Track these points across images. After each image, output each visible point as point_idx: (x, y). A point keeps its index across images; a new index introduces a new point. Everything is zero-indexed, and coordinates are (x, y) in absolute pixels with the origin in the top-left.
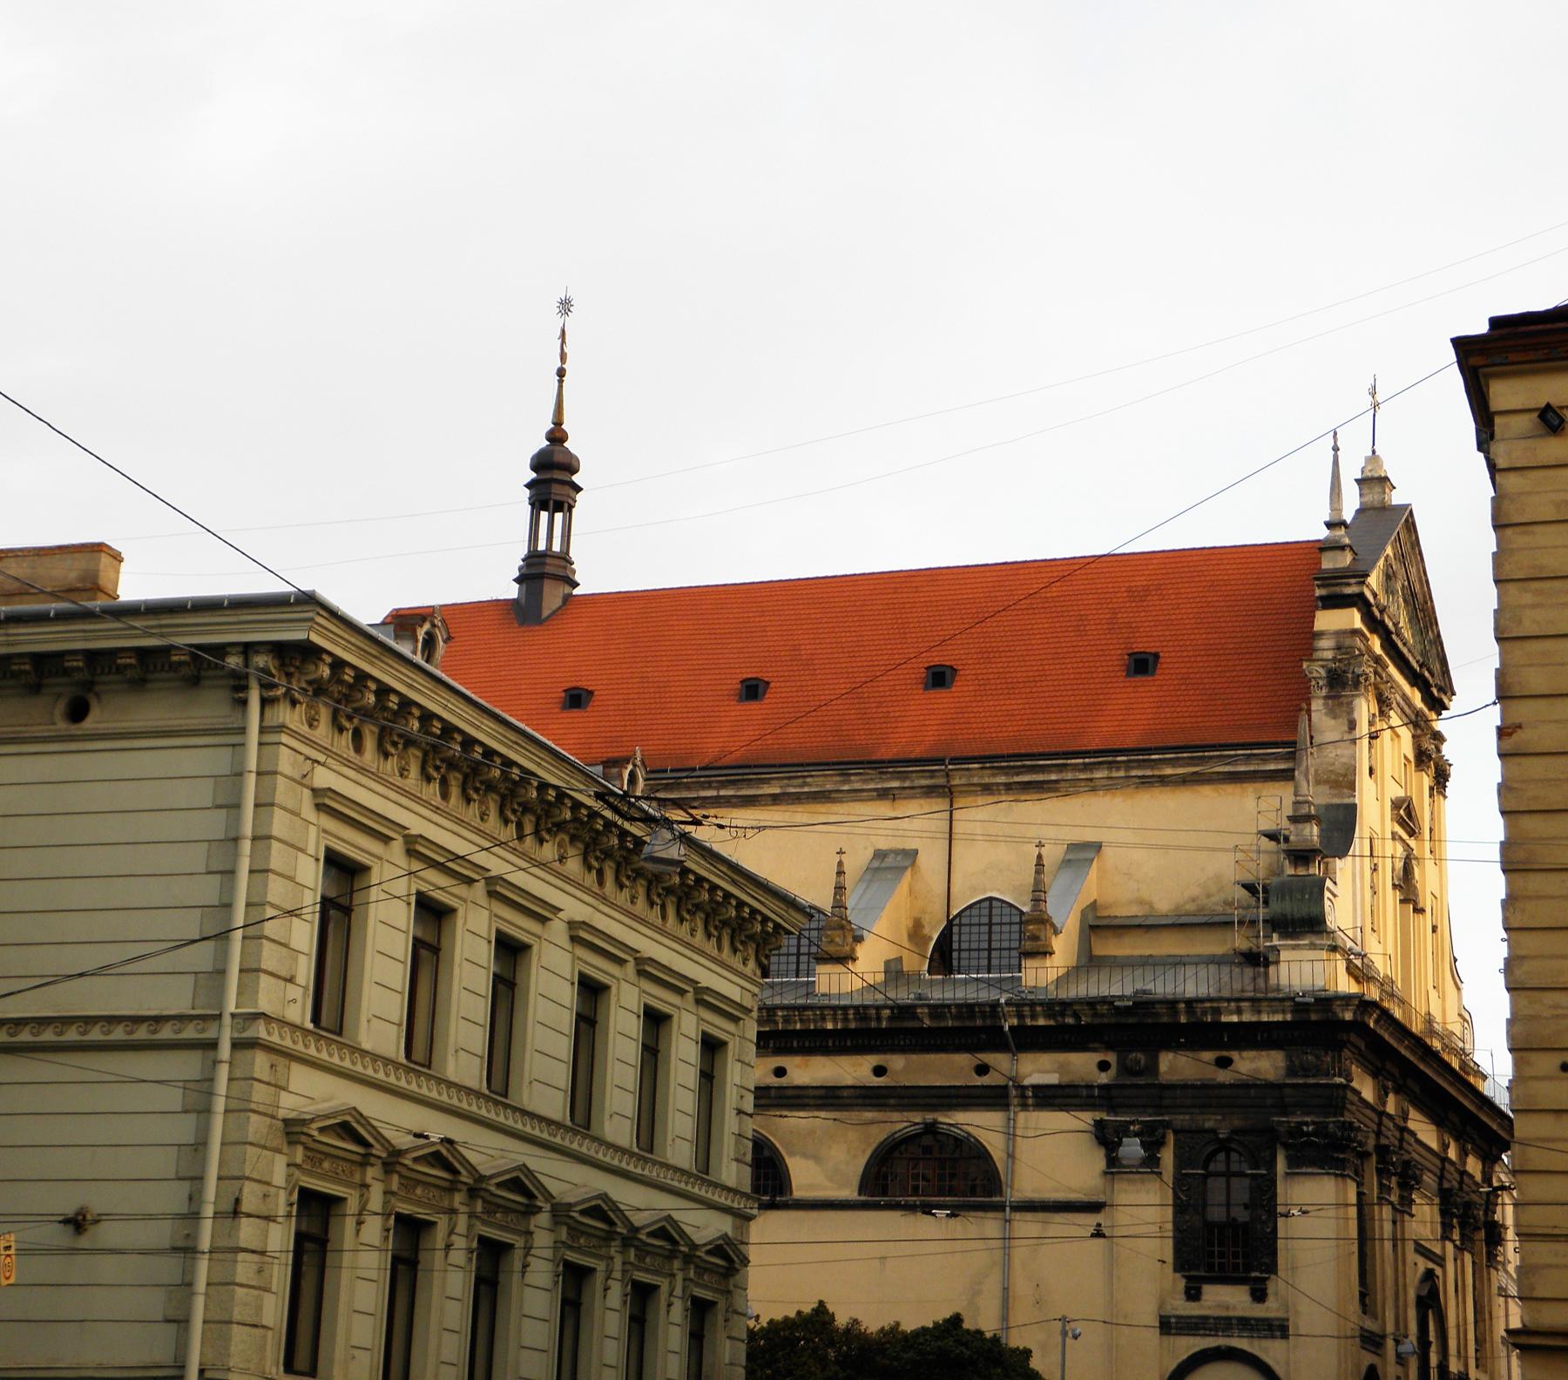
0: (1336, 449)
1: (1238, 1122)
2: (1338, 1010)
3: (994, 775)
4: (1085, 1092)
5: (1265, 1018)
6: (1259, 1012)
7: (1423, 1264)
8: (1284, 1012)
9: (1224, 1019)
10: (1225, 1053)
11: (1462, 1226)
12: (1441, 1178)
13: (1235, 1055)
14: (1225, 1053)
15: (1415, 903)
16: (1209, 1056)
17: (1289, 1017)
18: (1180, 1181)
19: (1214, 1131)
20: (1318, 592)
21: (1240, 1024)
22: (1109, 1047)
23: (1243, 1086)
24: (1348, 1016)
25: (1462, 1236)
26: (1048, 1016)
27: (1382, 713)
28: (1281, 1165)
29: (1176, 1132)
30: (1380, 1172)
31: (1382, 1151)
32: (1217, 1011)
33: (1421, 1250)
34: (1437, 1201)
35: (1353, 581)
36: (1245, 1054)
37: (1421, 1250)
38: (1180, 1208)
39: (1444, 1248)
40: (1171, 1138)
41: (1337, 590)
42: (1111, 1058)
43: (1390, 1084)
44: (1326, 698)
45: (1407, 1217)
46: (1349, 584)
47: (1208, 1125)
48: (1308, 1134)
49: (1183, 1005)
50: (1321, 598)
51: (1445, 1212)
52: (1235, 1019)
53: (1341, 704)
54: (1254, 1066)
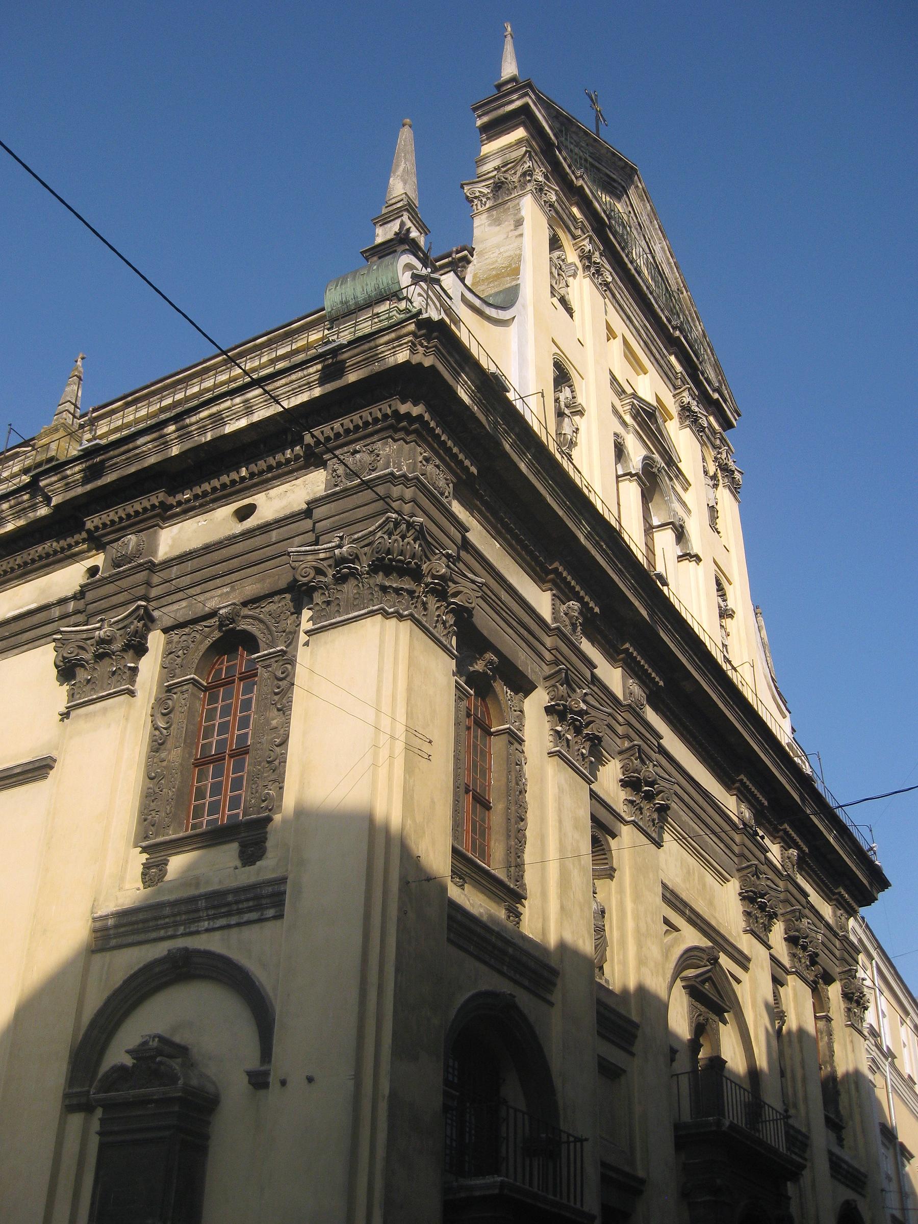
1: (251, 589)
3: (136, 411)
4: (56, 612)
7: (691, 938)
8: (309, 386)
9: (228, 429)
13: (259, 499)
16: (225, 512)
17: (317, 392)
18: (163, 706)
19: (213, 614)
20: (479, 123)
21: (252, 426)
22: (97, 543)
23: (265, 528)
24: (402, 356)
26: (18, 515)
29: (165, 631)
32: (218, 420)
33: (672, 898)
35: (515, 96)
38: (157, 745)
40: (156, 640)
41: (501, 111)
42: (99, 560)
44: (490, 209)
47: (211, 604)
48: (341, 561)
50: (485, 128)
52: (243, 423)
53: (505, 211)
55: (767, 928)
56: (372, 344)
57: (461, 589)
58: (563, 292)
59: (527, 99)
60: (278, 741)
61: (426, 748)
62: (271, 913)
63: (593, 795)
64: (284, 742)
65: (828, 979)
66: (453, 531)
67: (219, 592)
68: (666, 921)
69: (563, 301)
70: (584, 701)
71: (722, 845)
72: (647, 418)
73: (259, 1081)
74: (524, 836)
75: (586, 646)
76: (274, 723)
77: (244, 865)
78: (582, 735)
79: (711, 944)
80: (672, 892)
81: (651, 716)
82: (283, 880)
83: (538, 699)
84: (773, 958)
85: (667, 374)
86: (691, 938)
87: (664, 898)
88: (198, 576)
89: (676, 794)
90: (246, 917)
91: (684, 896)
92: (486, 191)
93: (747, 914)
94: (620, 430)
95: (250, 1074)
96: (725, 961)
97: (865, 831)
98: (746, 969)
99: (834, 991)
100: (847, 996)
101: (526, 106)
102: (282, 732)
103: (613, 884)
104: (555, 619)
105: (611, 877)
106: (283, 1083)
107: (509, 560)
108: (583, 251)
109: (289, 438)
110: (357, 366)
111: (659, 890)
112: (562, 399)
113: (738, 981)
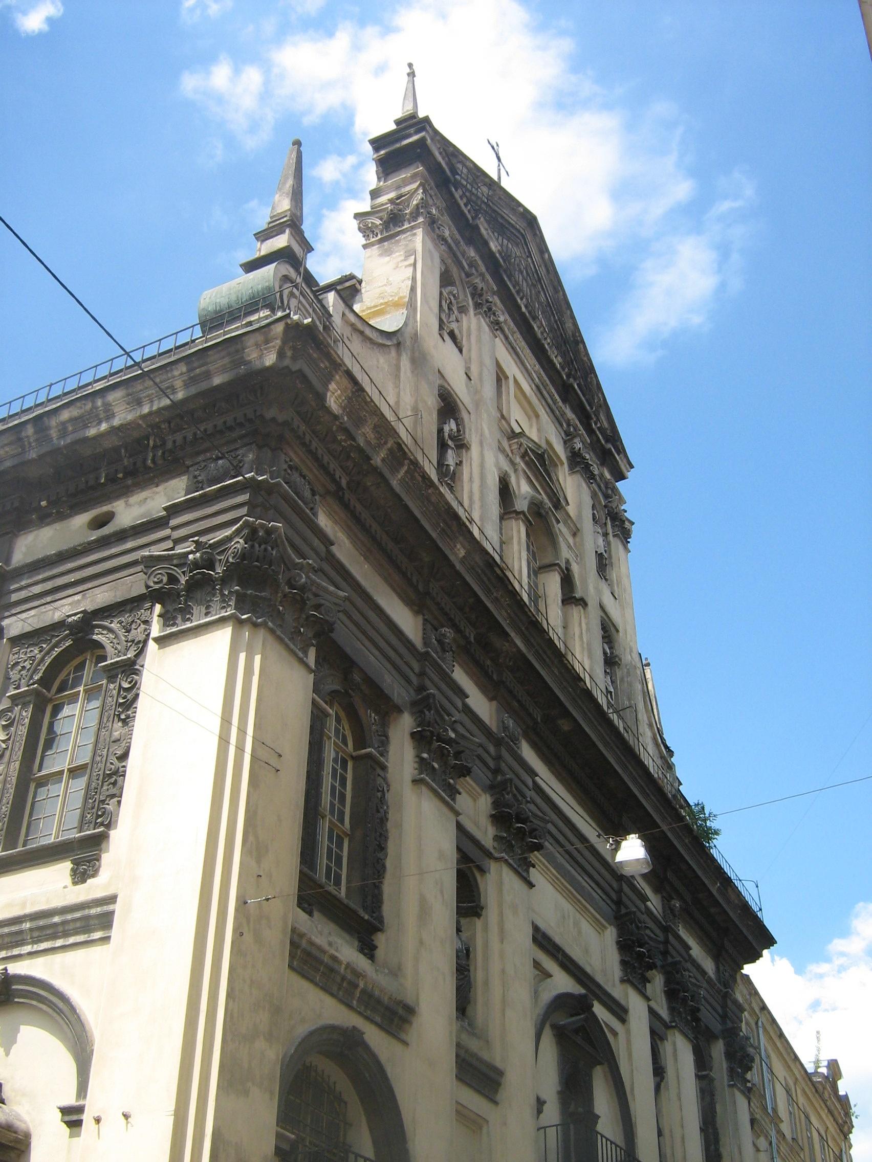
0: (412, 74)
2: (252, 354)
5: (146, 410)
6: (139, 403)
7: (562, 983)
9: (92, 432)
10: (105, 509)
11: (672, 994)
12: (619, 903)
13: (118, 506)
14: (105, 509)
15: (567, 581)
16: (81, 520)
17: (180, 395)
21: (114, 430)
24: (270, 359)
25: (672, 1009)
27: (477, 306)
28: (156, 630)
30: (420, 738)
31: (422, 705)
33: (542, 940)
34: (611, 934)
35: (412, 130)
36: (134, 499)
37: (542, 940)
39: (627, 995)
41: (398, 145)
43: (448, 632)
45: (509, 878)
46: (410, 136)
49: (30, 430)
51: (625, 946)
52: (104, 426)
54: (142, 510)
55: (646, 980)
56: (239, 346)
57: (323, 602)
58: (454, 326)
59: (423, 134)
60: (119, 753)
61: (274, 761)
62: (97, 935)
63: (460, 827)
64: (124, 756)
65: (711, 1036)
66: (316, 542)
67: (70, 600)
68: (537, 964)
69: (452, 335)
70: (454, 730)
71: (599, 891)
72: (539, 462)
73: (73, 1117)
74: (384, 866)
75: (460, 676)
76: (116, 734)
77: (75, 883)
78: (444, 764)
79: (583, 991)
80: (545, 936)
81: (528, 753)
82: (112, 899)
83: (405, 724)
84: (651, 1011)
85: (558, 419)
86: (562, 983)
87: (535, 940)
88: (49, 585)
89: (550, 833)
90: (71, 940)
91: (557, 939)
92: (378, 222)
93: (623, 963)
94: (506, 466)
95: (66, 1111)
96: (598, 1010)
97: (750, 886)
98: (623, 1021)
99: (718, 1050)
100: (729, 1056)
101: (423, 140)
102: (123, 744)
103: (479, 923)
104: (426, 643)
105: (478, 915)
106: (98, 1120)
107: (378, 580)
108: (475, 288)
109: (151, 443)
110: (224, 370)
111: (530, 931)
112: (446, 428)
113: (615, 1034)
